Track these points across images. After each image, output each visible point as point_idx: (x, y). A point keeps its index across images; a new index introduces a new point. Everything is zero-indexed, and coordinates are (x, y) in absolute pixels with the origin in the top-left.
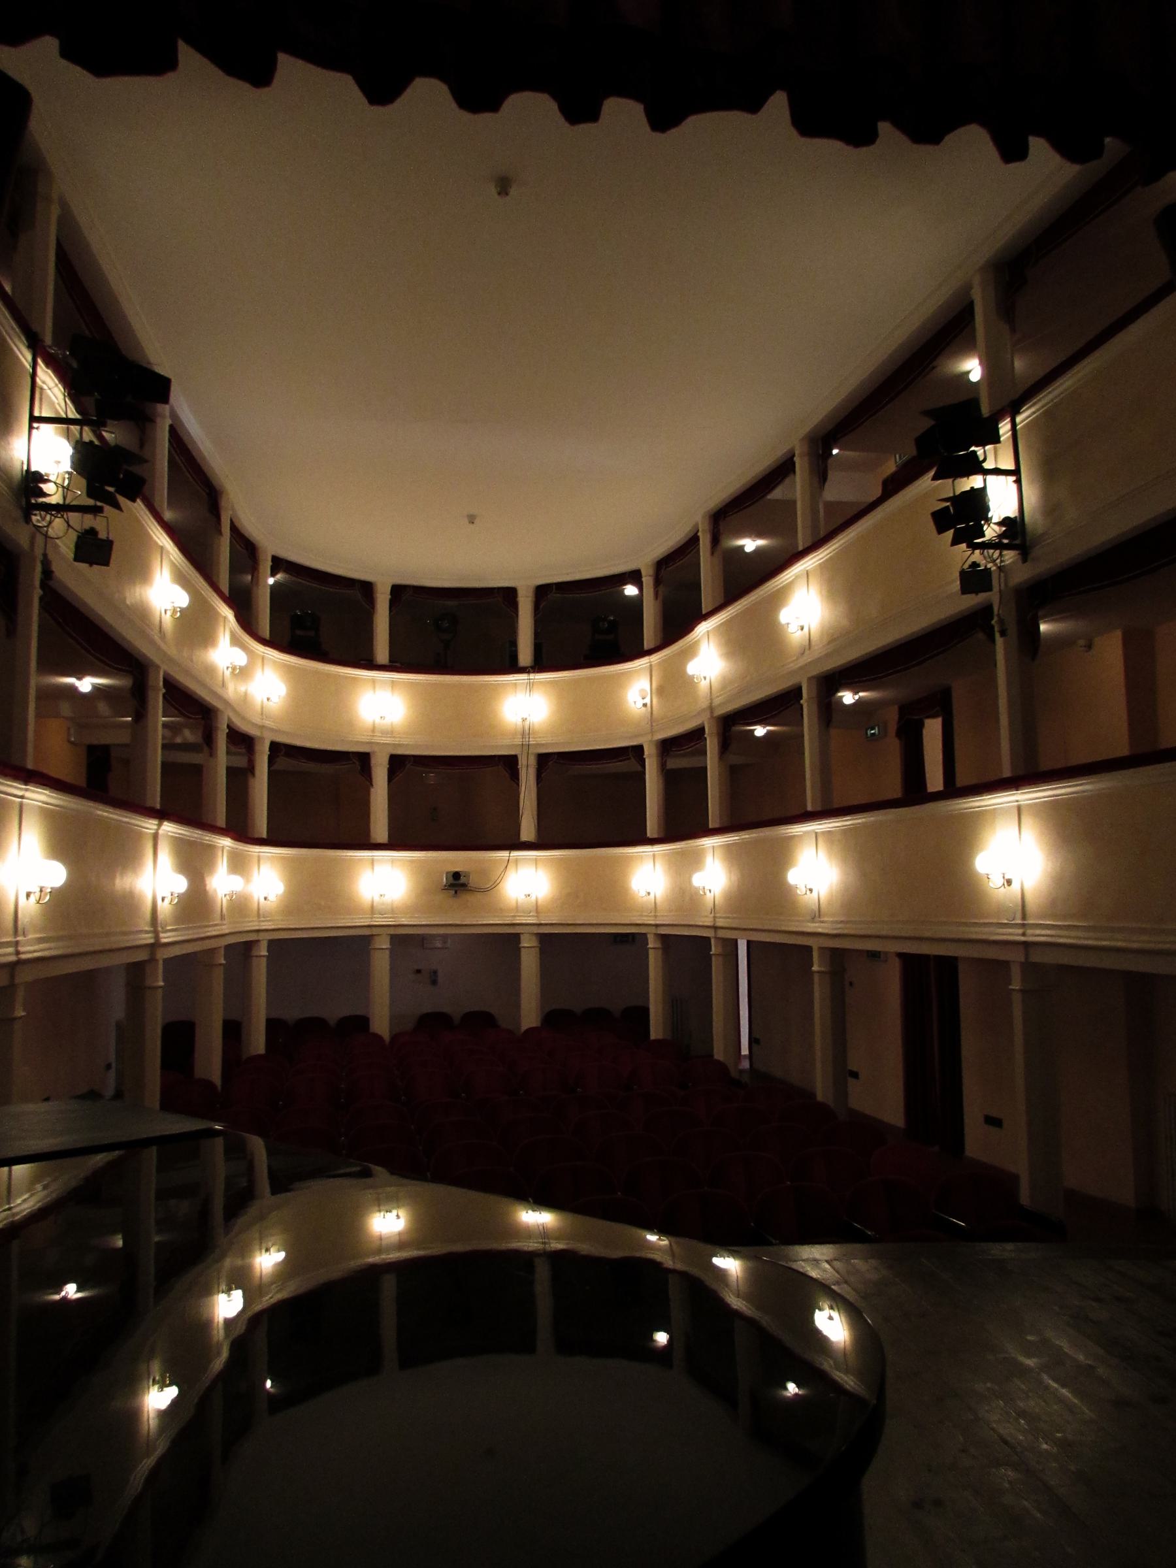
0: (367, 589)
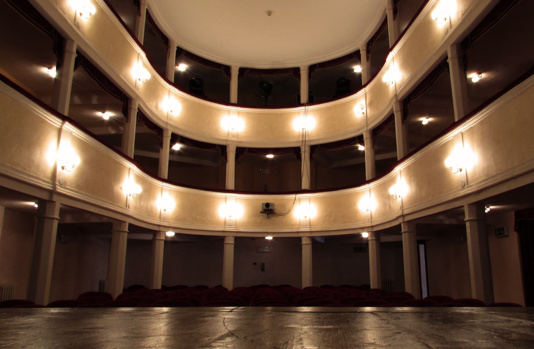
0: (227, 69)
